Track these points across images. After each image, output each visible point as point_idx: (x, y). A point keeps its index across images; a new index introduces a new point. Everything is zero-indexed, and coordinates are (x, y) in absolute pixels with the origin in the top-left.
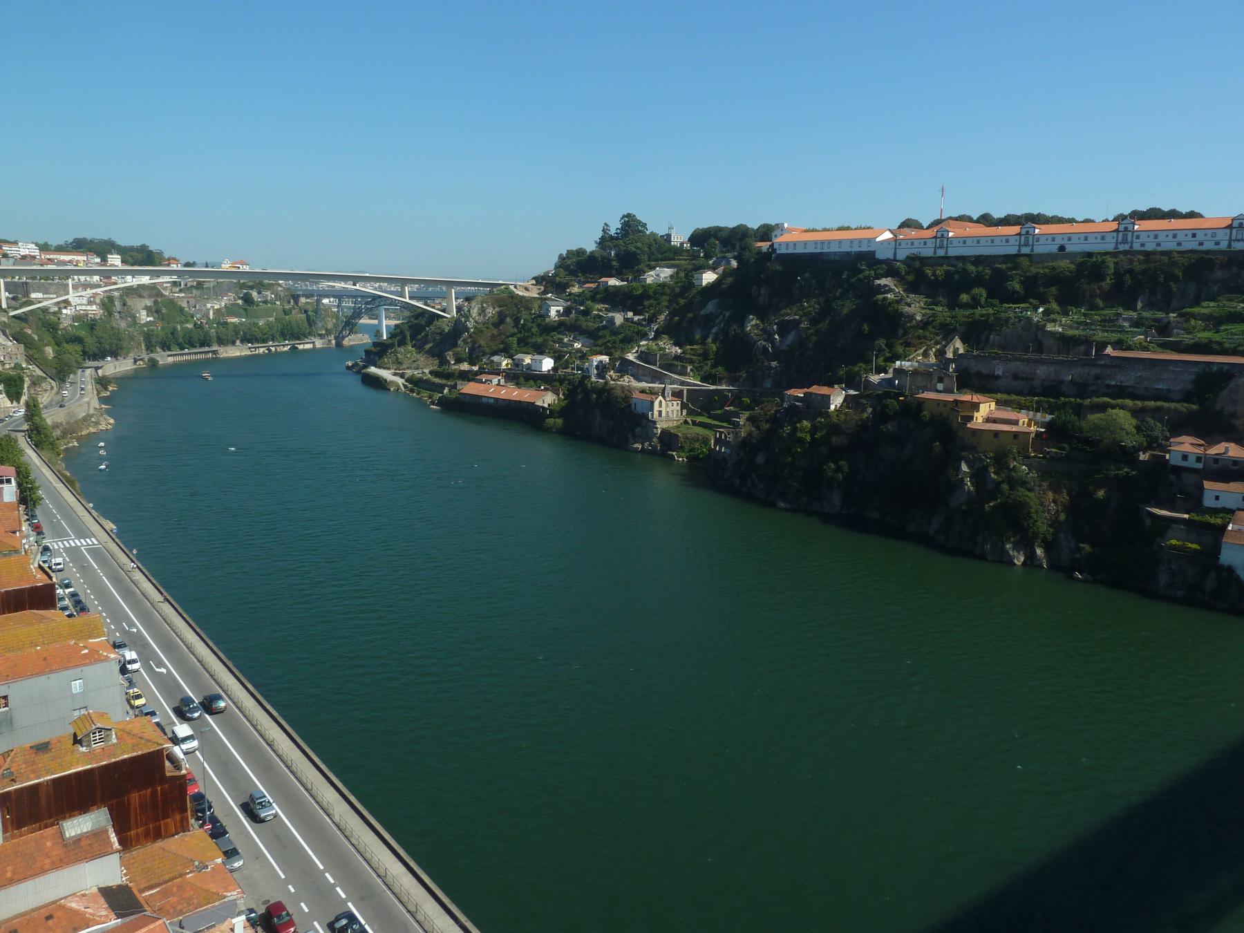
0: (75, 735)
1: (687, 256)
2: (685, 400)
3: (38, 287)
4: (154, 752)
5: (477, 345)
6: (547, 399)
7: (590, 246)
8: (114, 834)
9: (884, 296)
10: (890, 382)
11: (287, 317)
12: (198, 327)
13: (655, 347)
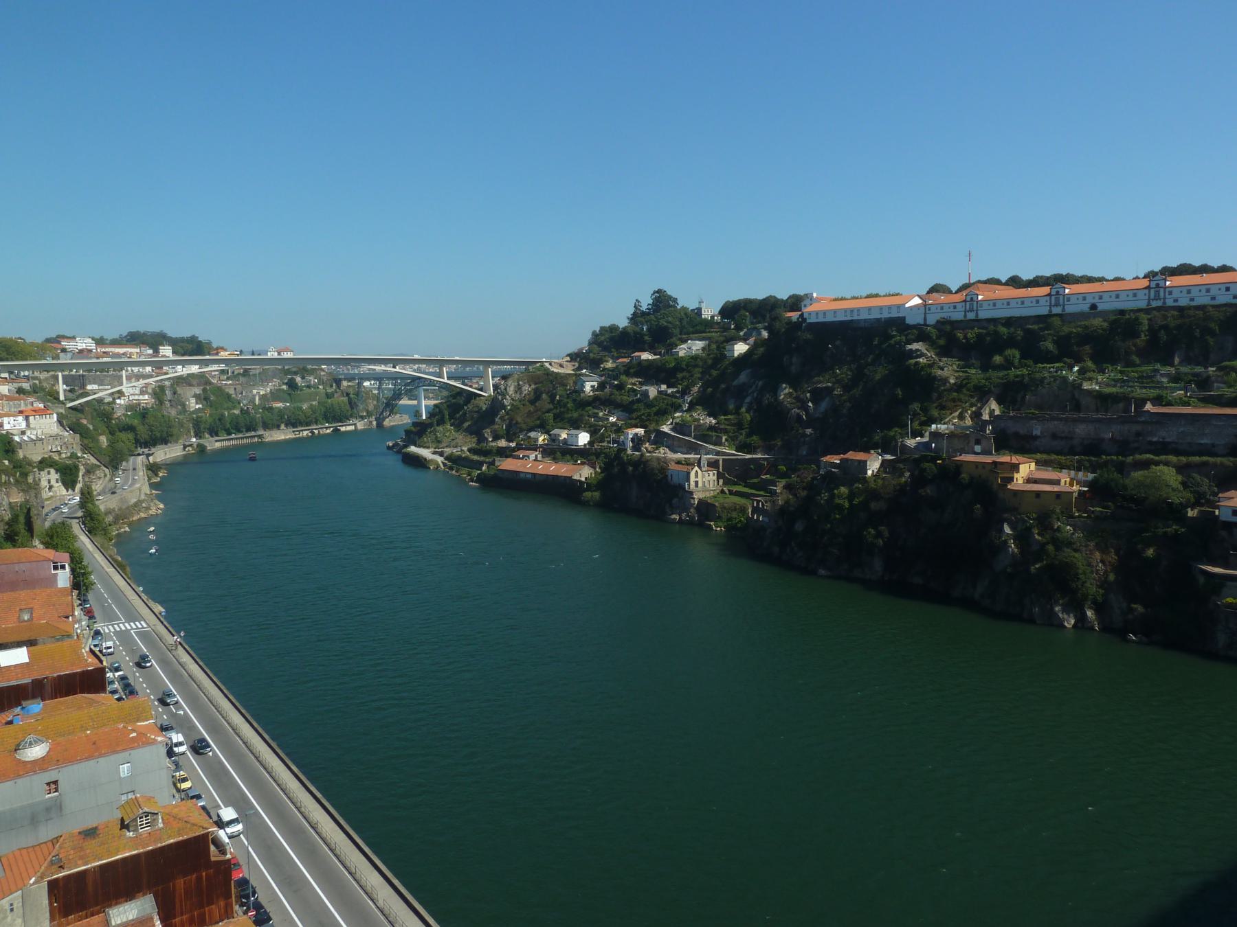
0: (122, 820)
1: (718, 328)
2: (721, 470)
3: (94, 379)
4: (199, 836)
5: (514, 422)
6: (584, 473)
7: (623, 323)
8: (159, 922)
10: (926, 445)
11: (329, 401)
12: (244, 412)
13: (689, 419)
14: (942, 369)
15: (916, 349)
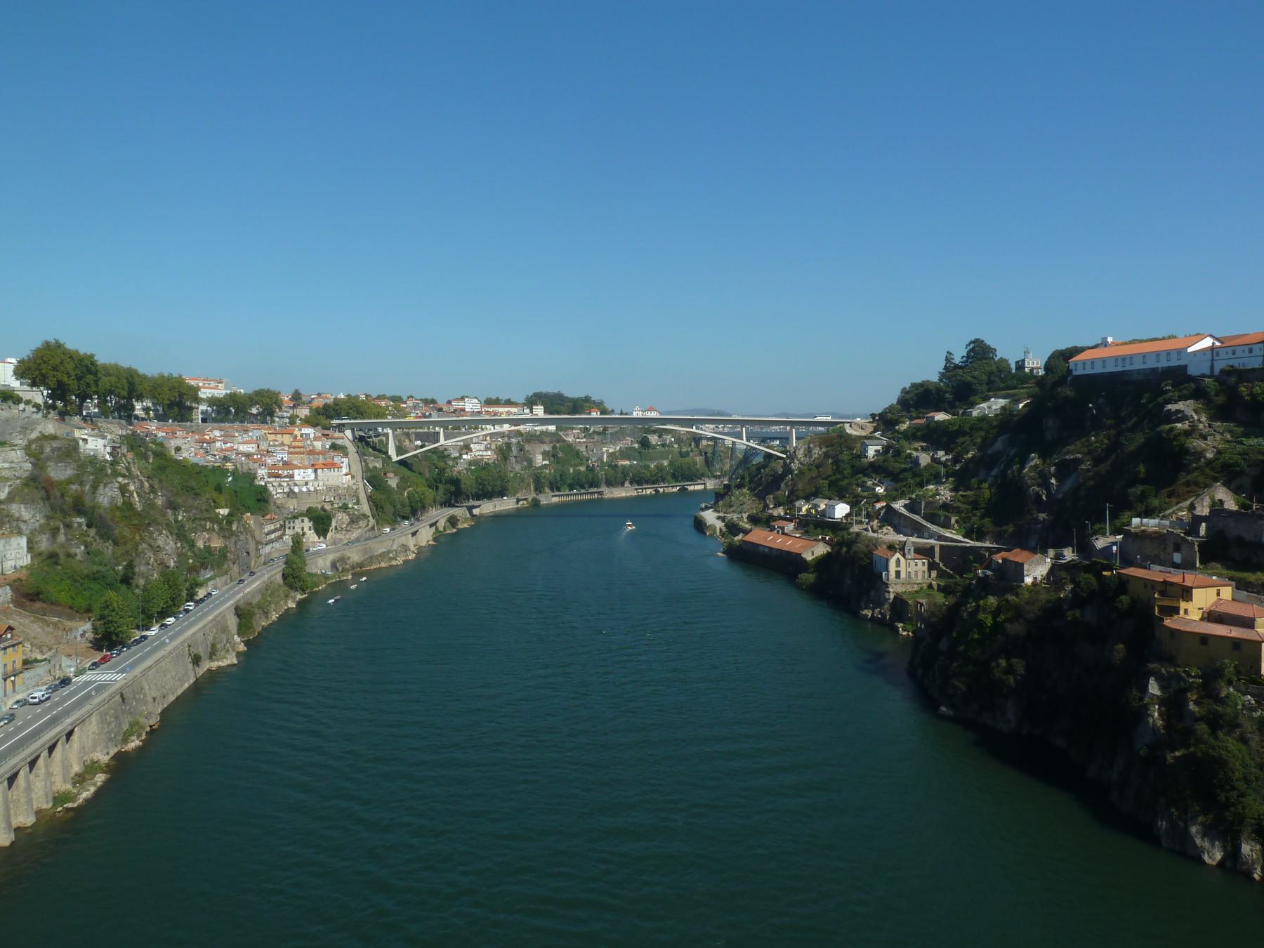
2: (937, 559)
5: (795, 488)
9: (1170, 426)
12: (590, 469)
14: (1205, 438)
15: (1177, 410)
